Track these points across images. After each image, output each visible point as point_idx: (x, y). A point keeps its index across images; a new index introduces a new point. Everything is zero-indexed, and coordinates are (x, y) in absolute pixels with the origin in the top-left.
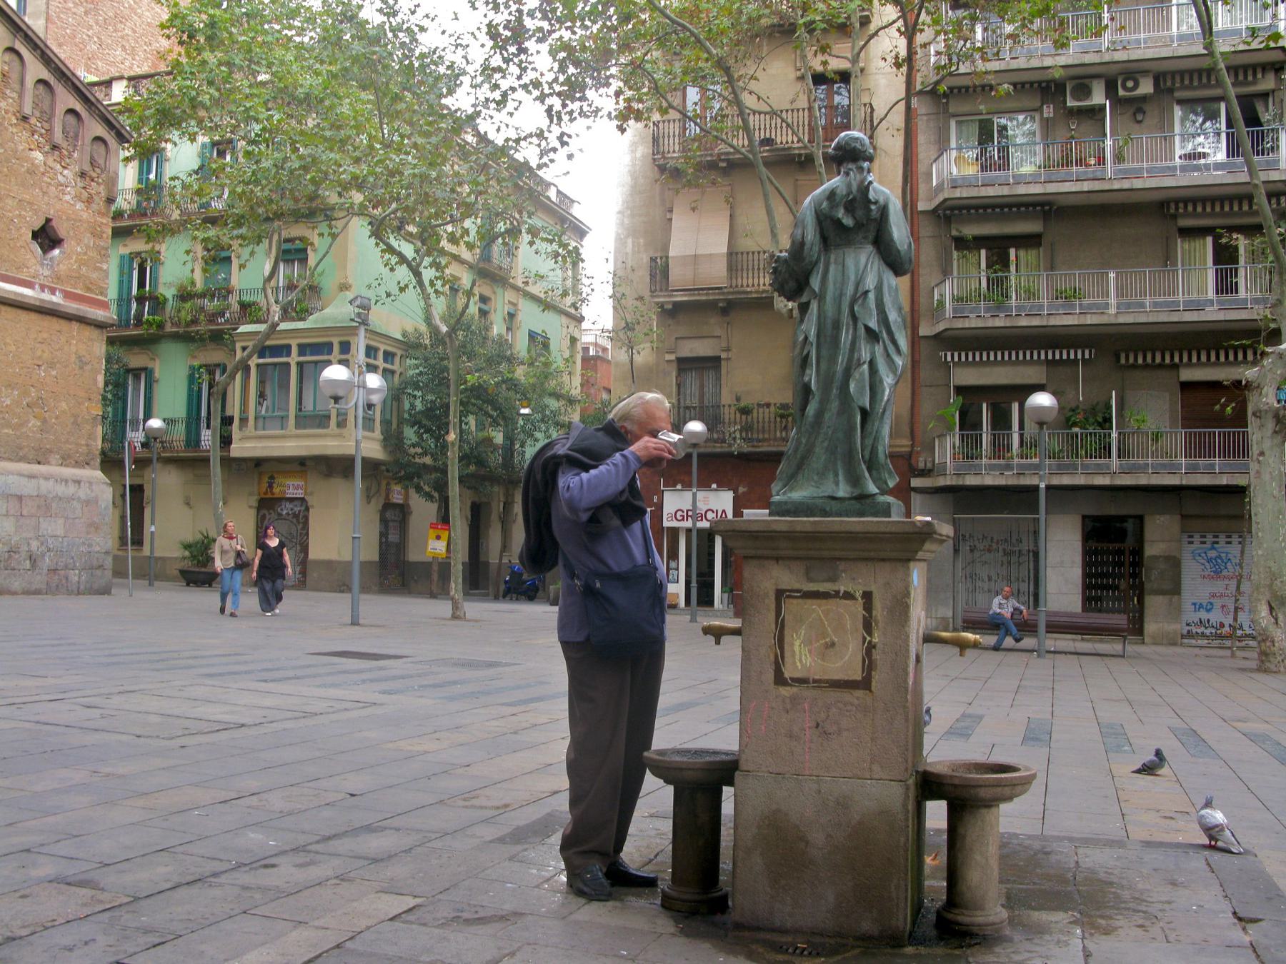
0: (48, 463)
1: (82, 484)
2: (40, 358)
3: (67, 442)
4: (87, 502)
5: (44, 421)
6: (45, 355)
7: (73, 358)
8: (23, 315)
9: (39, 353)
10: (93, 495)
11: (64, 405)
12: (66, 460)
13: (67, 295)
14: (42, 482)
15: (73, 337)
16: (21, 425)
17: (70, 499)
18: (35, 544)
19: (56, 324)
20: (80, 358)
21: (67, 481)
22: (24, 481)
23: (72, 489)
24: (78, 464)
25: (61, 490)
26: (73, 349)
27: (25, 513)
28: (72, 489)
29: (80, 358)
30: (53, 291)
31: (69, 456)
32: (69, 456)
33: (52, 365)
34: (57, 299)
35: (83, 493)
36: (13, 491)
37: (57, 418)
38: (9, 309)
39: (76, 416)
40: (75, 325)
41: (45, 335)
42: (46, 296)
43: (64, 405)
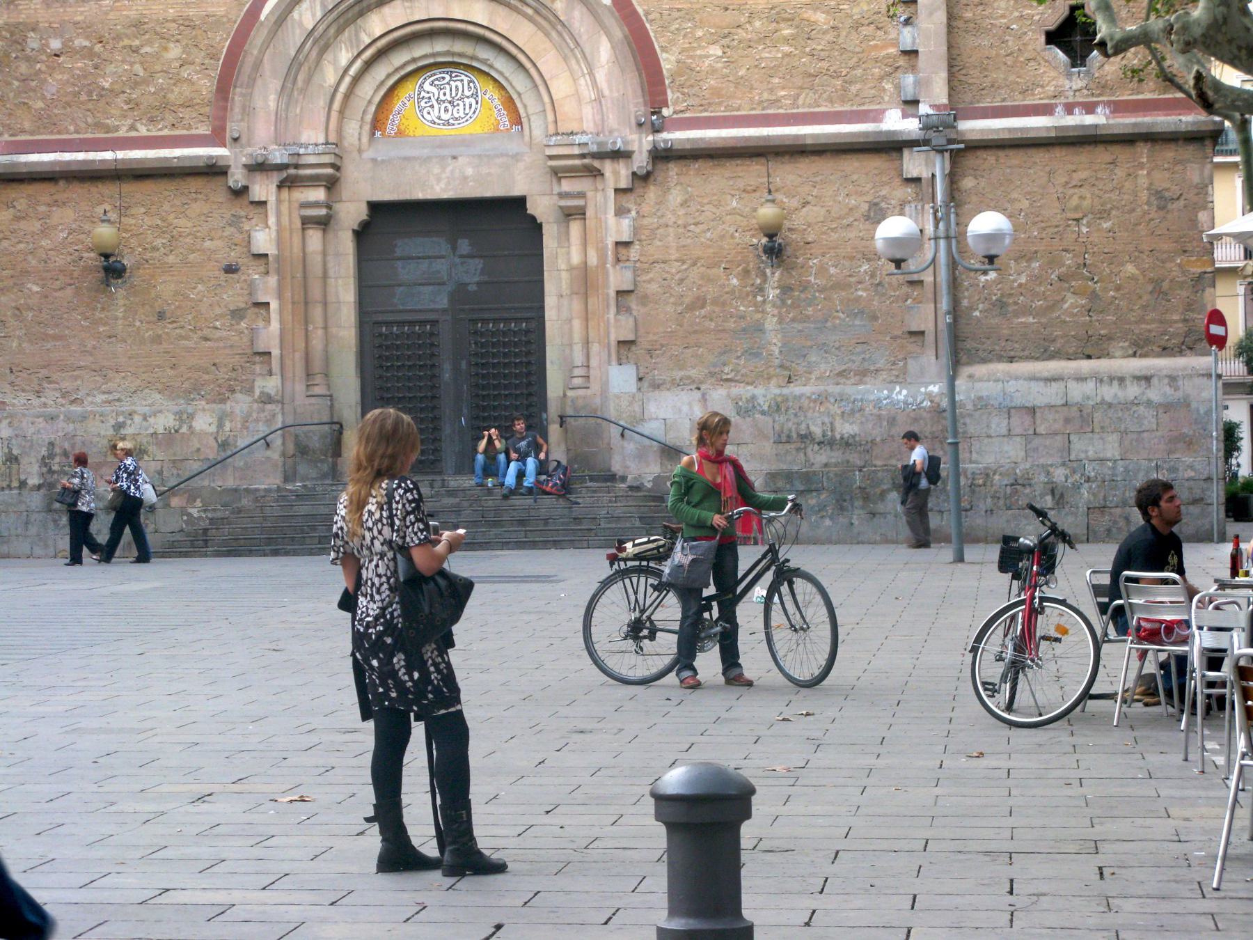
0: (1108, 355)
1: (1155, 381)
2: (1076, 208)
3: (1142, 320)
4: (1167, 407)
5: (1094, 296)
6: (1086, 203)
7: (1144, 195)
8: (1040, 156)
9: (1075, 201)
10: (1179, 394)
11: (1130, 269)
12: (1140, 348)
13: (1118, 108)
14: (1072, 385)
15: (1141, 166)
16: (1051, 308)
17: (1135, 403)
18: (1059, 474)
19: (1103, 155)
20: (1159, 194)
21: (1121, 380)
22: (1036, 387)
23: (1133, 390)
24: (1166, 351)
25: (1109, 392)
26: (1143, 181)
27: (1041, 429)
28: (1133, 390)
29: (1159, 194)
30: (1090, 108)
31: (1147, 341)
32: (1147, 341)
33: (1103, 214)
34: (1099, 119)
35: (1155, 394)
36: (1018, 401)
37: (1118, 289)
38: (1011, 153)
39: (1157, 282)
40: (1143, 150)
41: (1083, 175)
42: (1089, 120)
43: (1130, 269)
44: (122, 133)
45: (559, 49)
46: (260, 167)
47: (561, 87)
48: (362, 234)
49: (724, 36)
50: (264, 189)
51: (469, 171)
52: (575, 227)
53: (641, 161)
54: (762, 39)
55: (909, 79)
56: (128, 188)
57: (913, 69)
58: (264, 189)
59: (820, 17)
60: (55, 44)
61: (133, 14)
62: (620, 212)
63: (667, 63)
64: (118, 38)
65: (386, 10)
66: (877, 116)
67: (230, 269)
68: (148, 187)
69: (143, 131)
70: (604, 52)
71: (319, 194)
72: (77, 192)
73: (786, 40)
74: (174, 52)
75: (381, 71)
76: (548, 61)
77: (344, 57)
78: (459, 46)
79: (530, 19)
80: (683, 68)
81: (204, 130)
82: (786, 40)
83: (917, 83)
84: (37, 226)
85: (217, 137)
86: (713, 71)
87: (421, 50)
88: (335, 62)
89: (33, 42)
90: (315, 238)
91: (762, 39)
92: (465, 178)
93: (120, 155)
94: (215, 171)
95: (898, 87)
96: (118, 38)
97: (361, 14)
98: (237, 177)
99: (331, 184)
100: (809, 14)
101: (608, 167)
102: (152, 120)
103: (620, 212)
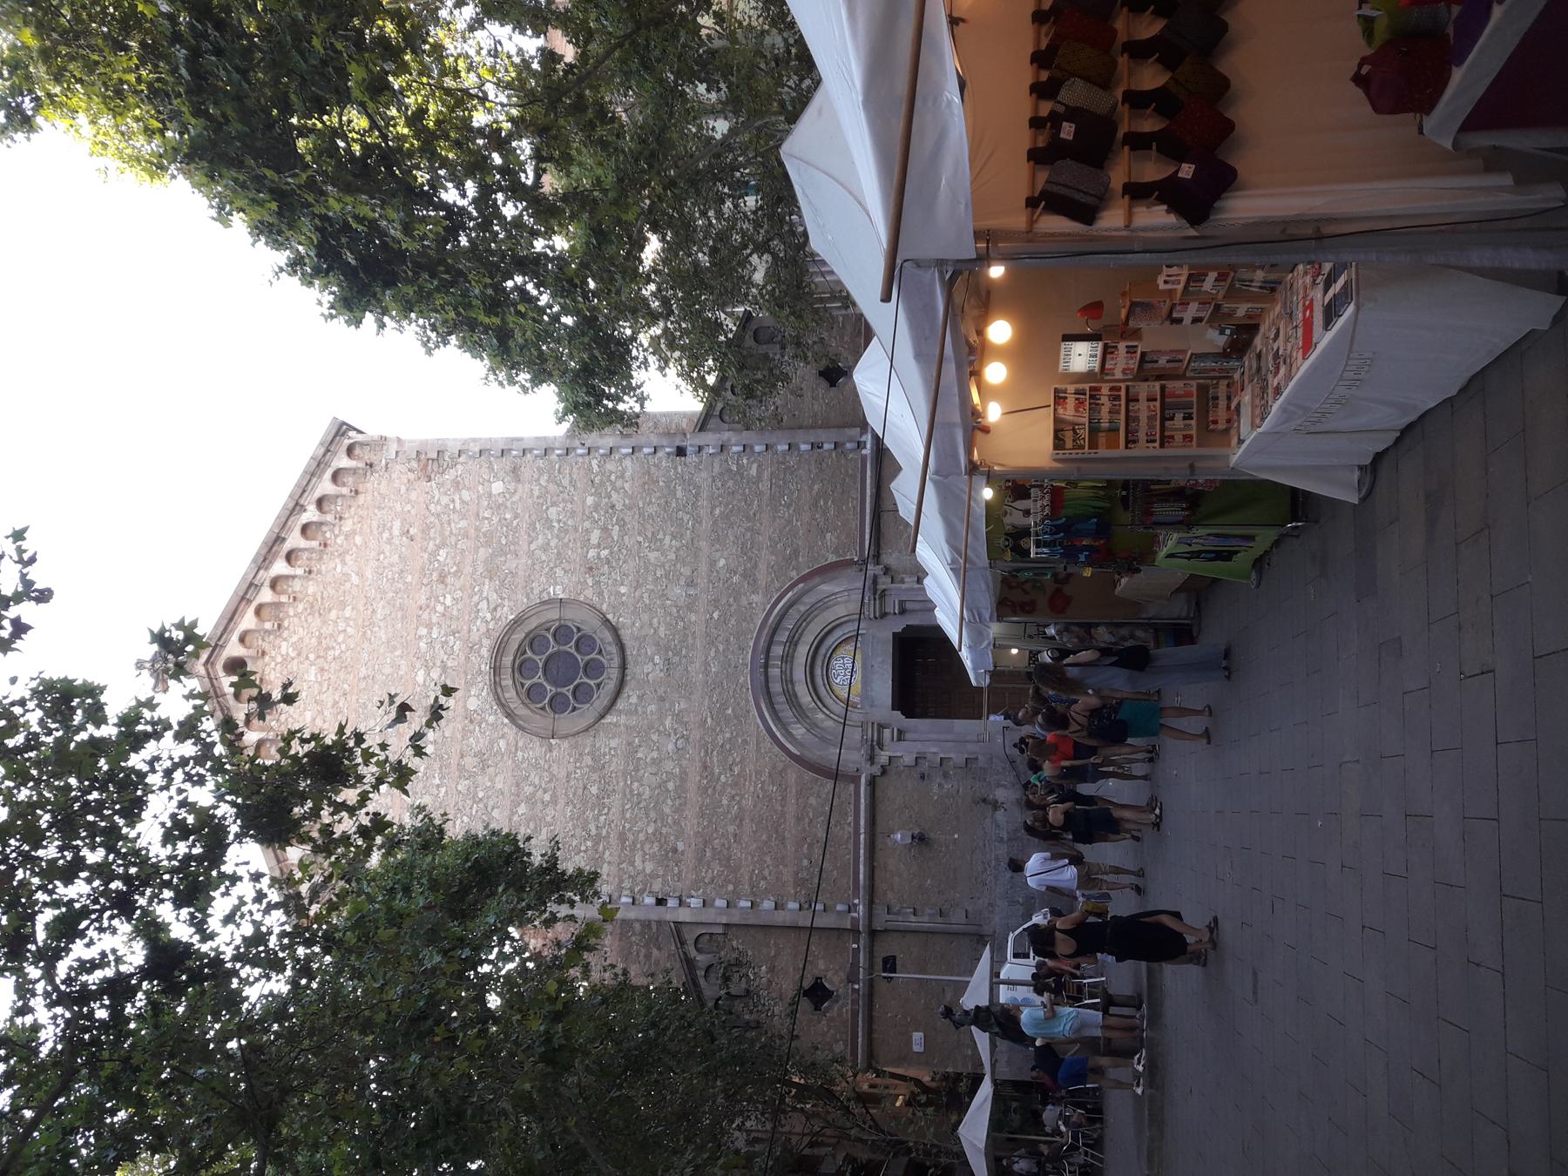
44: (851, 830)
45: (823, 610)
46: (872, 759)
47: (840, 611)
48: (909, 713)
49: (822, 533)
50: (883, 758)
51: (880, 659)
52: (909, 606)
53: (878, 570)
54: (824, 513)
55: (848, 445)
56: (879, 829)
57: (844, 444)
58: (883, 758)
59: (816, 487)
60: (805, 862)
61: (793, 821)
62: (902, 581)
63: (832, 558)
64: (804, 830)
65: (799, 695)
66: (864, 458)
67: (923, 777)
68: (879, 818)
69: (851, 819)
70: (826, 588)
71: (887, 733)
72: (879, 854)
73: (826, 503)
74: (812, 801)
75: (828, 701)
76: (828, 616)
77: (821, 716)
78: (819, 662)
79: (808, 624)
80: (836, 551)
81: (852, 787)
82: (826, 503)
83: (850, 441)
84: (897, 879)
85: (855, 780)
86: (838, 538)
87: (818, 671)
88: (823, 721)
89: (804, 875)
90: (908, 736)
91: (824, 513)
92: (883, 661)
93: (862, 830)
94: (872, 782)
95: (851, 450)
96: (804, 830)
97: (800, 706)
98: (876, 770)
99: (881, 727)
100: (814, 493)
101: (881, 587)
102: (846, 814)
103: (902, 581)
